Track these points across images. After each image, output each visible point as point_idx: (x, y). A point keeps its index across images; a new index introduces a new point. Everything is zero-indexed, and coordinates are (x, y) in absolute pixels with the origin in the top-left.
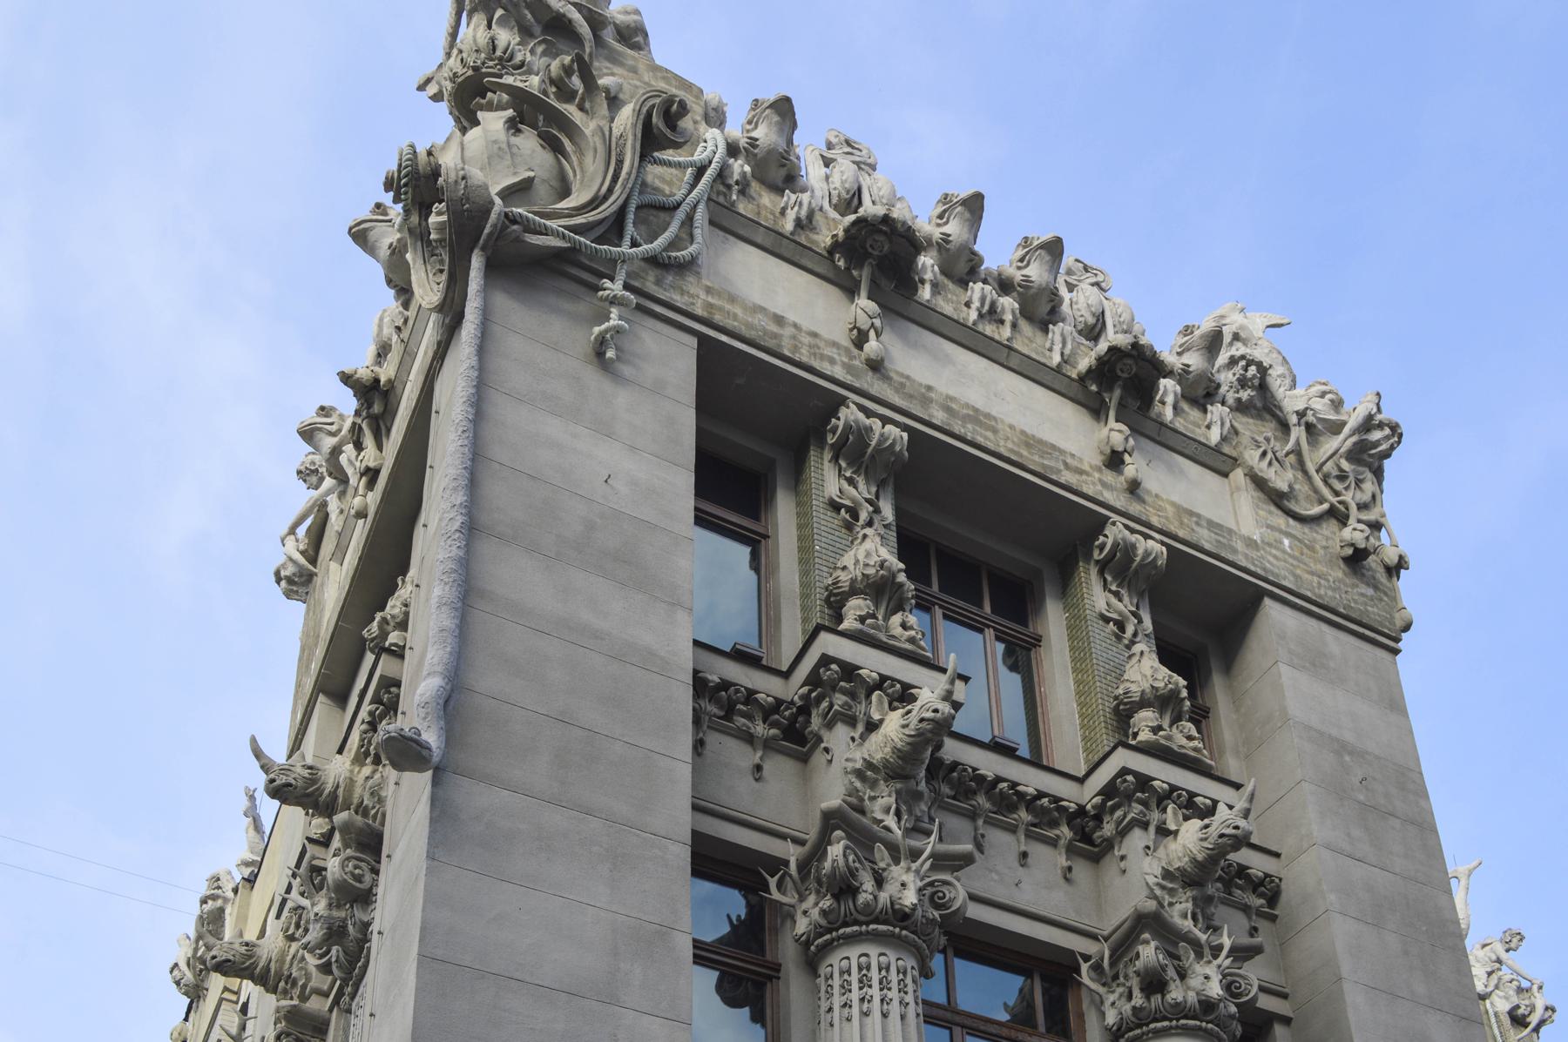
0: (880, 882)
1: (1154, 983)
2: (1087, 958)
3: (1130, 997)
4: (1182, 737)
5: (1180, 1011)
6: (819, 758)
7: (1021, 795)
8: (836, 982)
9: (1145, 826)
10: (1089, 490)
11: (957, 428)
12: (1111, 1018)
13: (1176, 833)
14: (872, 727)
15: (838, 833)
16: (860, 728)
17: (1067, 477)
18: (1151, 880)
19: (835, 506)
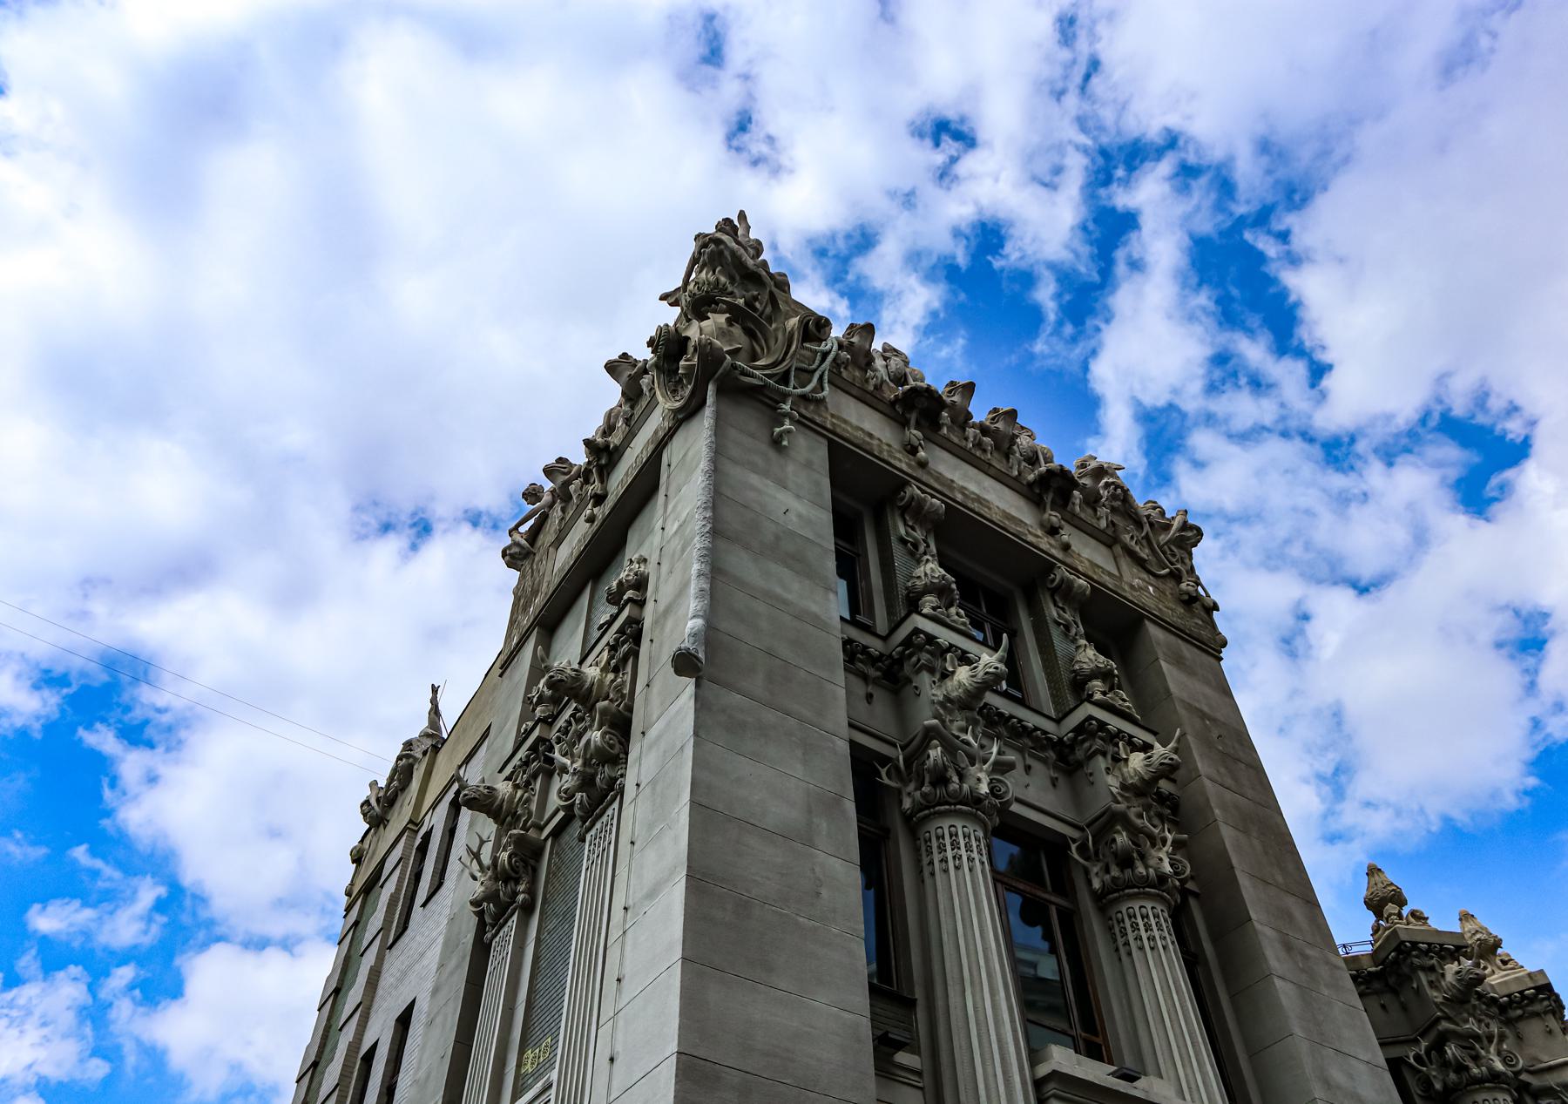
0: (962, 777)
1: (1126, 861)
2: (1074, 841)
3: (1107, 871)
4: (1123, 699)
5: (1146, 882)
6: (908, 691)
7: (1025, 728)
8: (935, 844)
9: (1104, 754)
11: (970, 505)
13: (1126, 760)
14: (945, 675)
15: (935, 742)
16: (938, 676)
17: (1030, 538)
18: (1115, 790)
19: (903, 541)
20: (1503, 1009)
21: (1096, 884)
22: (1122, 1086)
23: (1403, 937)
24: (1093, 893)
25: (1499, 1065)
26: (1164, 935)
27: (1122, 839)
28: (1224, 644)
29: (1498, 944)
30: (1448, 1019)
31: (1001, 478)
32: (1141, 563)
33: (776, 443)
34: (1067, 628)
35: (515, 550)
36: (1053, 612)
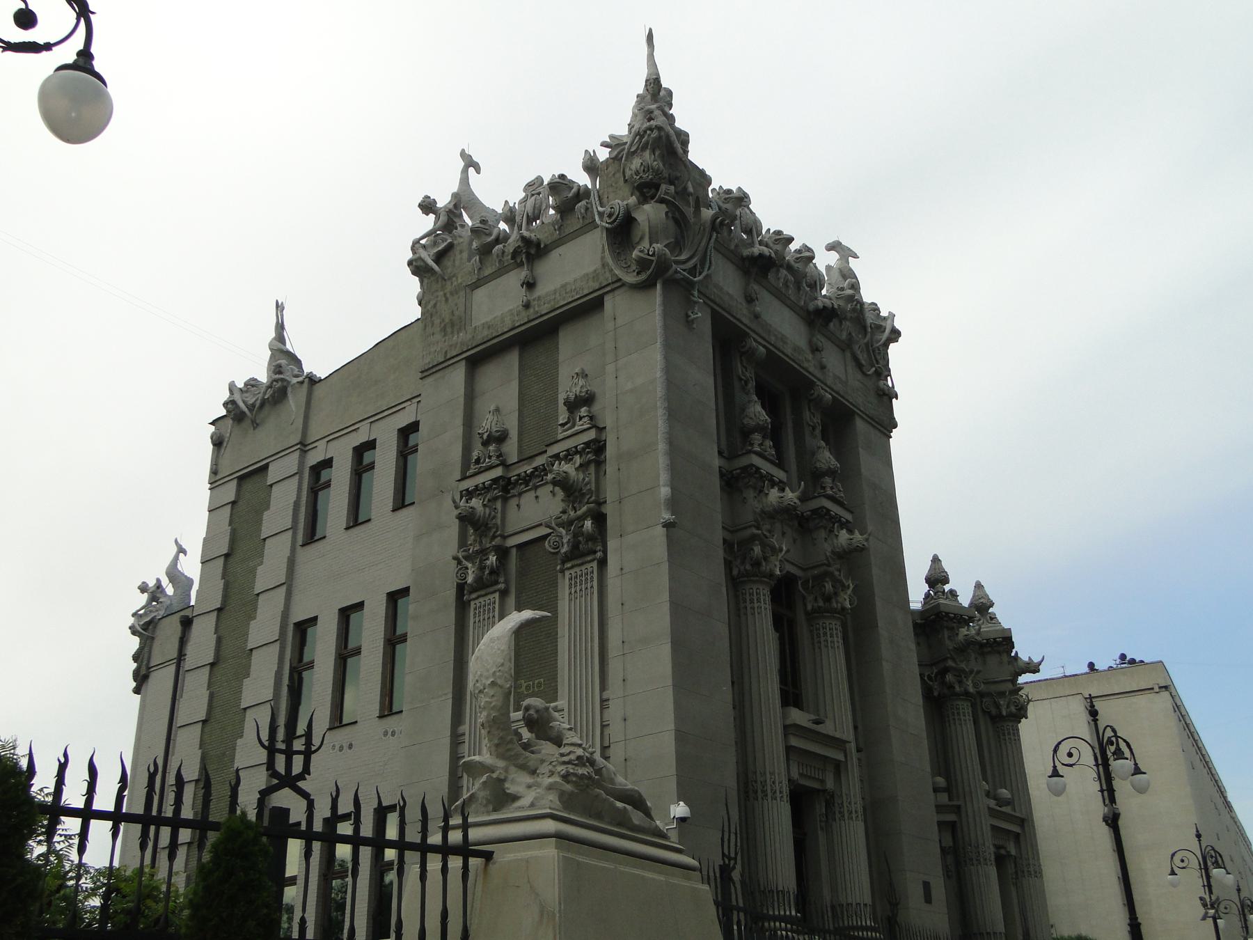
3: (816, 599)
9: (825, 528)
10: (811, 369)
12: (809, 607)
17: (806, 365)
20: (981, 645)
21: (809, 607)
22: (814, 727)
23: (942, 609)
24: (807, 613)
25: (971, 690)
26: (838, 641)
27: (829, 587)
28: (895, 426)
29: (992, 605)
30: (954, 660)
31: (792, 307)
32: (859, 366)
33: (689, 323)
34: (814, 428)
35: (420, 263)
36: (807, 415)
